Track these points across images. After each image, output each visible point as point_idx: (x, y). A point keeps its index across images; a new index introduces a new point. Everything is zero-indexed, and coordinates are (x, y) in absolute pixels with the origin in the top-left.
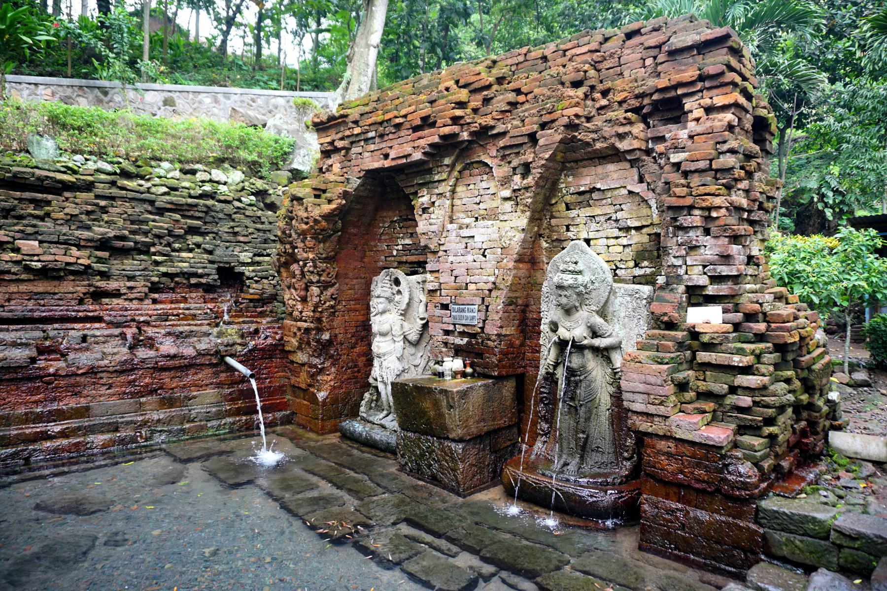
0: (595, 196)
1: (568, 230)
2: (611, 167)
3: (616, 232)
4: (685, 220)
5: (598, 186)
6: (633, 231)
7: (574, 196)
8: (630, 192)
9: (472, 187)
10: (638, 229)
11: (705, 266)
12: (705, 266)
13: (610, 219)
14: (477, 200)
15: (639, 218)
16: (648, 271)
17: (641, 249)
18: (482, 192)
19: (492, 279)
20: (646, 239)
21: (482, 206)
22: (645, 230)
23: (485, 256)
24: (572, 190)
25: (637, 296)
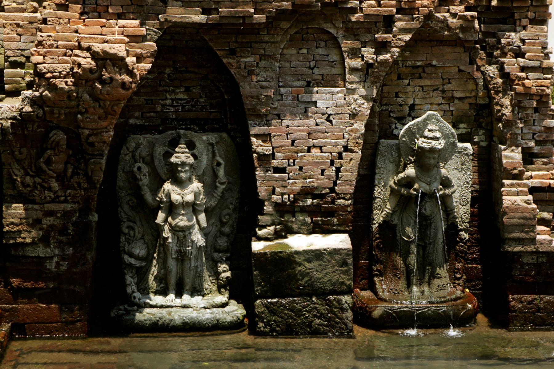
0: (428, 70)
1: (397, 96)
2: (448, 50)
3: (440, 100)
4: (526, 103)
5: (434, 63)
6: (456, 101)
7: (409, 69)
8: (460, 71)
9: (305, 51)
10: (460, 99)
11: (534, 134)
12: (534, 134)
13: (437, 89)
14: (312, 64)
15: (464, 91)
16: (464, 131)
17: (461, 114)
18: (318, 58)
19: (342, 142)
20: (467, 107)
21: (316, 71)
22: (466, 101)
23: (331, 122)
24: (409, 63)
25: (465, 152)
